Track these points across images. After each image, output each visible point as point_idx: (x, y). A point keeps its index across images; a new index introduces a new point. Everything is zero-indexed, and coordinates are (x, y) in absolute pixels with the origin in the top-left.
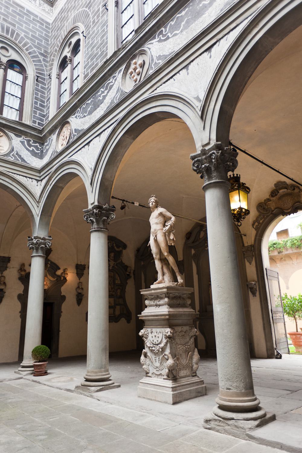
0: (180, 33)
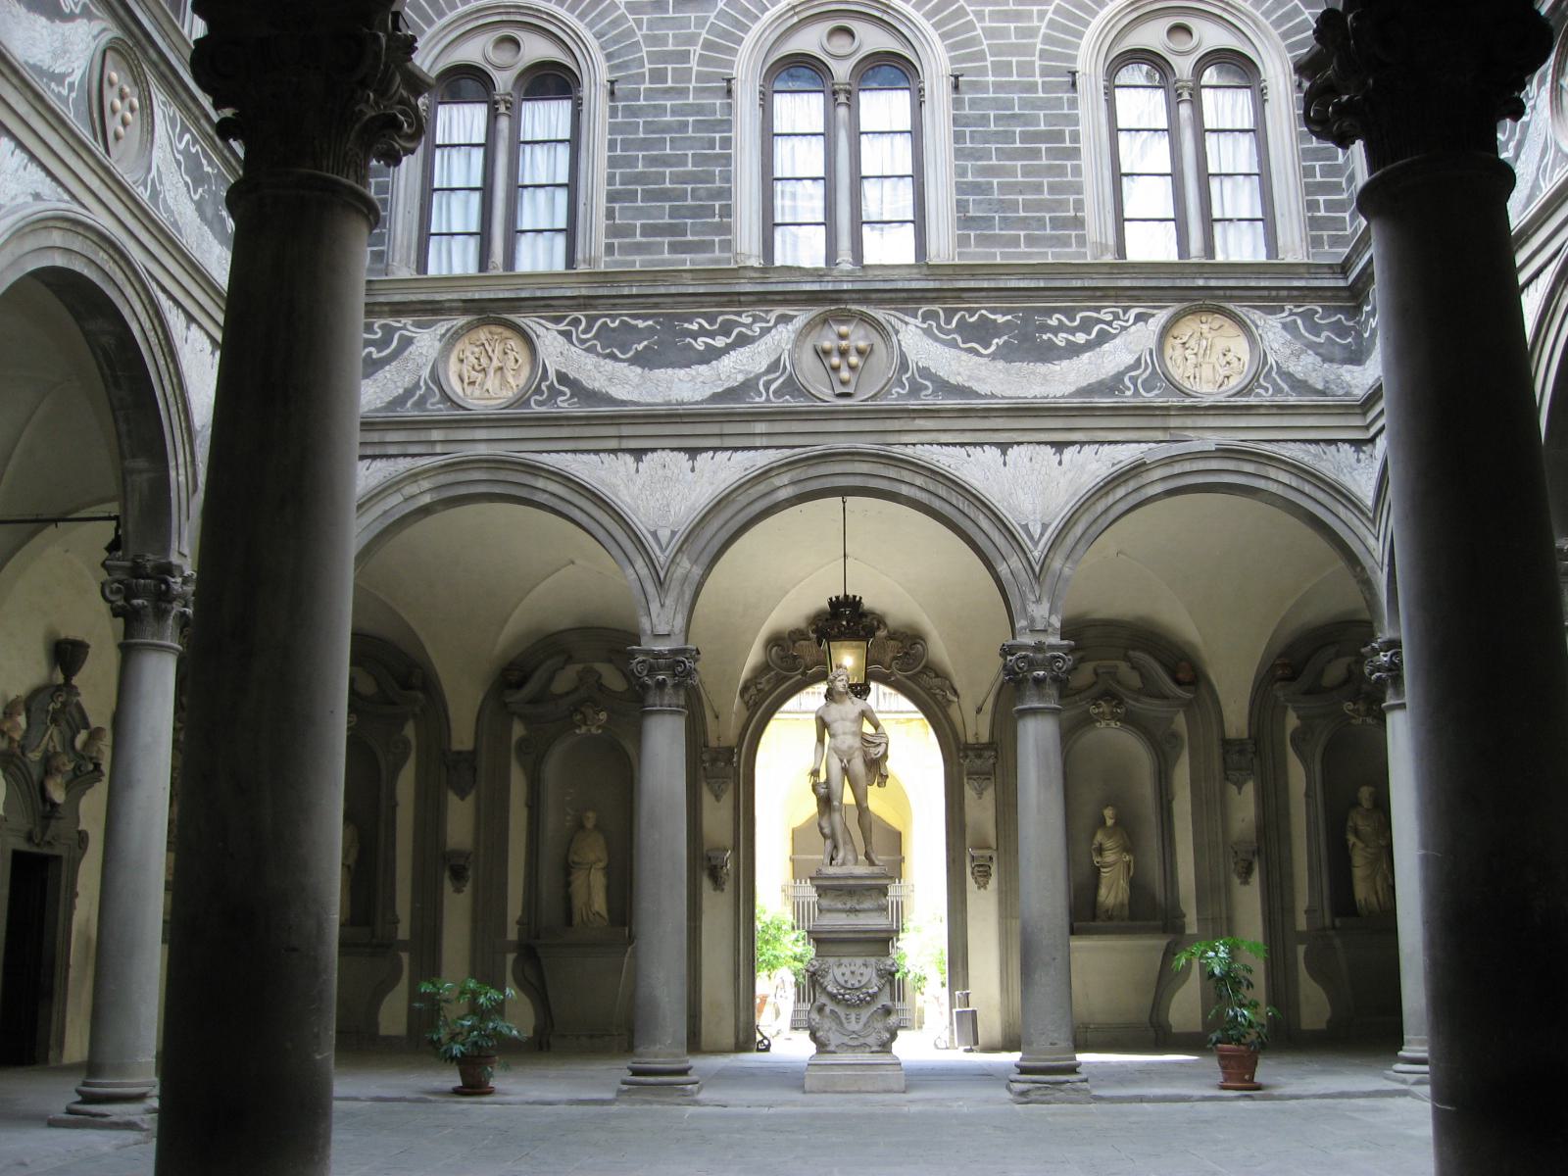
0: (988, 356)
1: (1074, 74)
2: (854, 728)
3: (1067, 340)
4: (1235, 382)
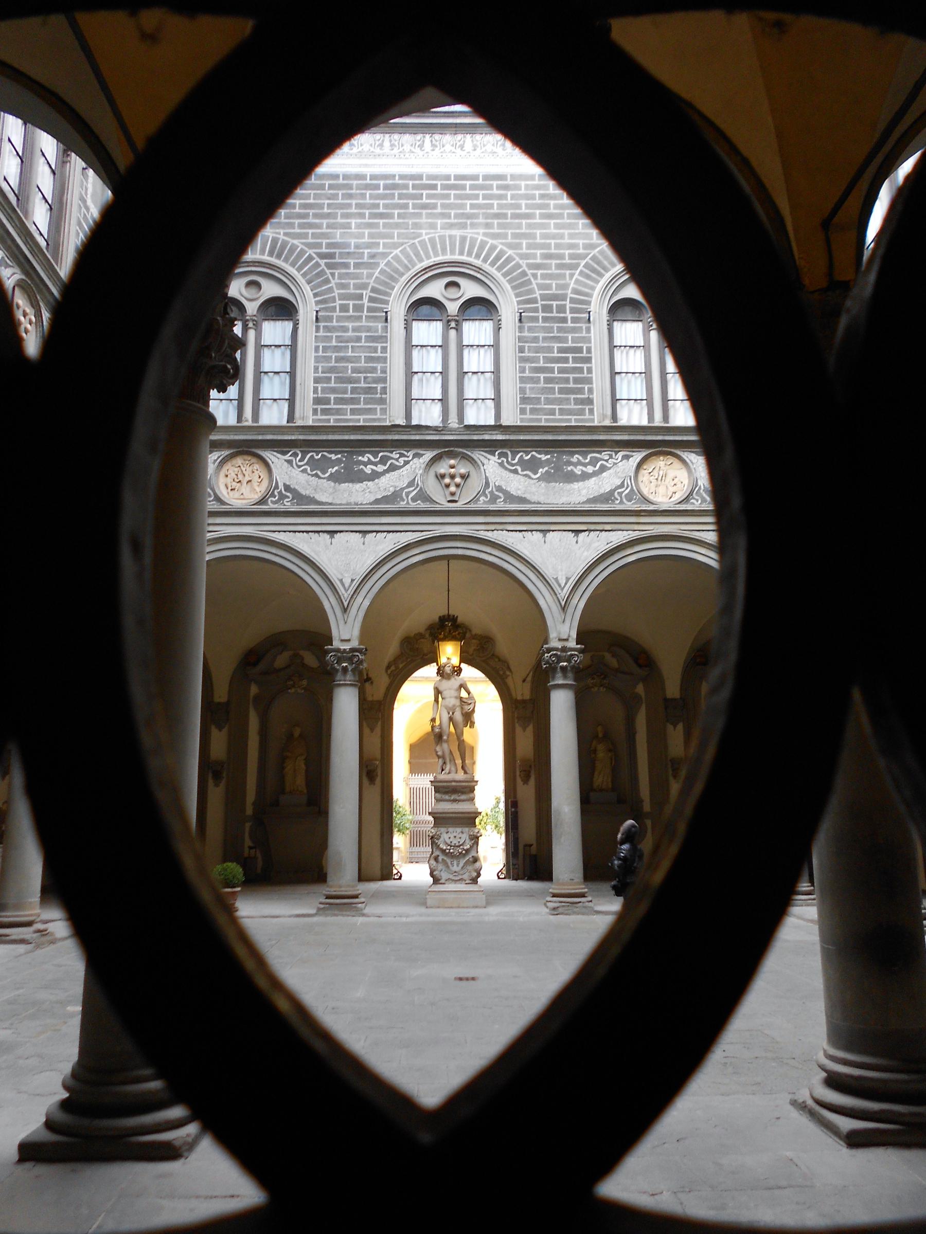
1: (589, 312)
2: (456, 694)
3: (582, 471)
4: (678, 497)
